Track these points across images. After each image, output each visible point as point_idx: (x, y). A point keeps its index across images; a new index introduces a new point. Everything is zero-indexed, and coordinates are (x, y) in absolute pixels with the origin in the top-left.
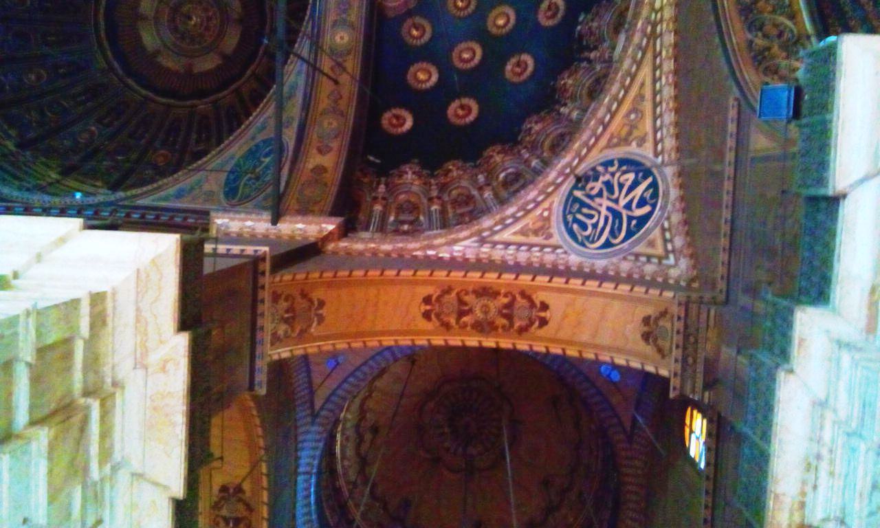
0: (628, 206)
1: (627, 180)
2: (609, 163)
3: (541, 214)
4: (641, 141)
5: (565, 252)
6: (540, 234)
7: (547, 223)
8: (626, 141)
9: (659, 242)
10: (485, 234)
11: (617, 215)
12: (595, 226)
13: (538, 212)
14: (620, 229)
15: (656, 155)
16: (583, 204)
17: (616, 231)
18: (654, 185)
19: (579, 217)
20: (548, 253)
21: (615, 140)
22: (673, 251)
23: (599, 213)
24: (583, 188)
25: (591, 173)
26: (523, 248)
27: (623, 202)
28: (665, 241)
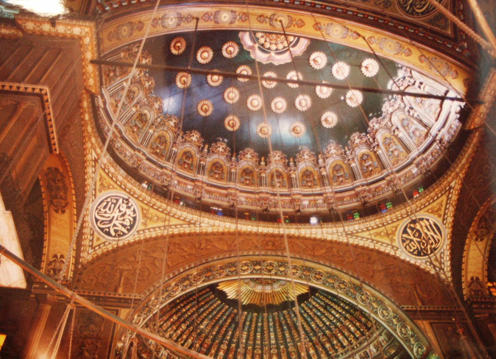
0: (115, 225)
2: (134, 211)
4: (145, 224)
8: (145, 216)
9: (99, 243)
11: (110, 221)
12: (106, 212)
14: (105, 224)
15: (138, 232)
16: (115, 204)
18: (124, 234)
19: (110, 204)
22: (95, 250)
23: (112, 213)
24: (123, 202)
25: (130, 204)
27: (117, 223)
28: (99, 245)
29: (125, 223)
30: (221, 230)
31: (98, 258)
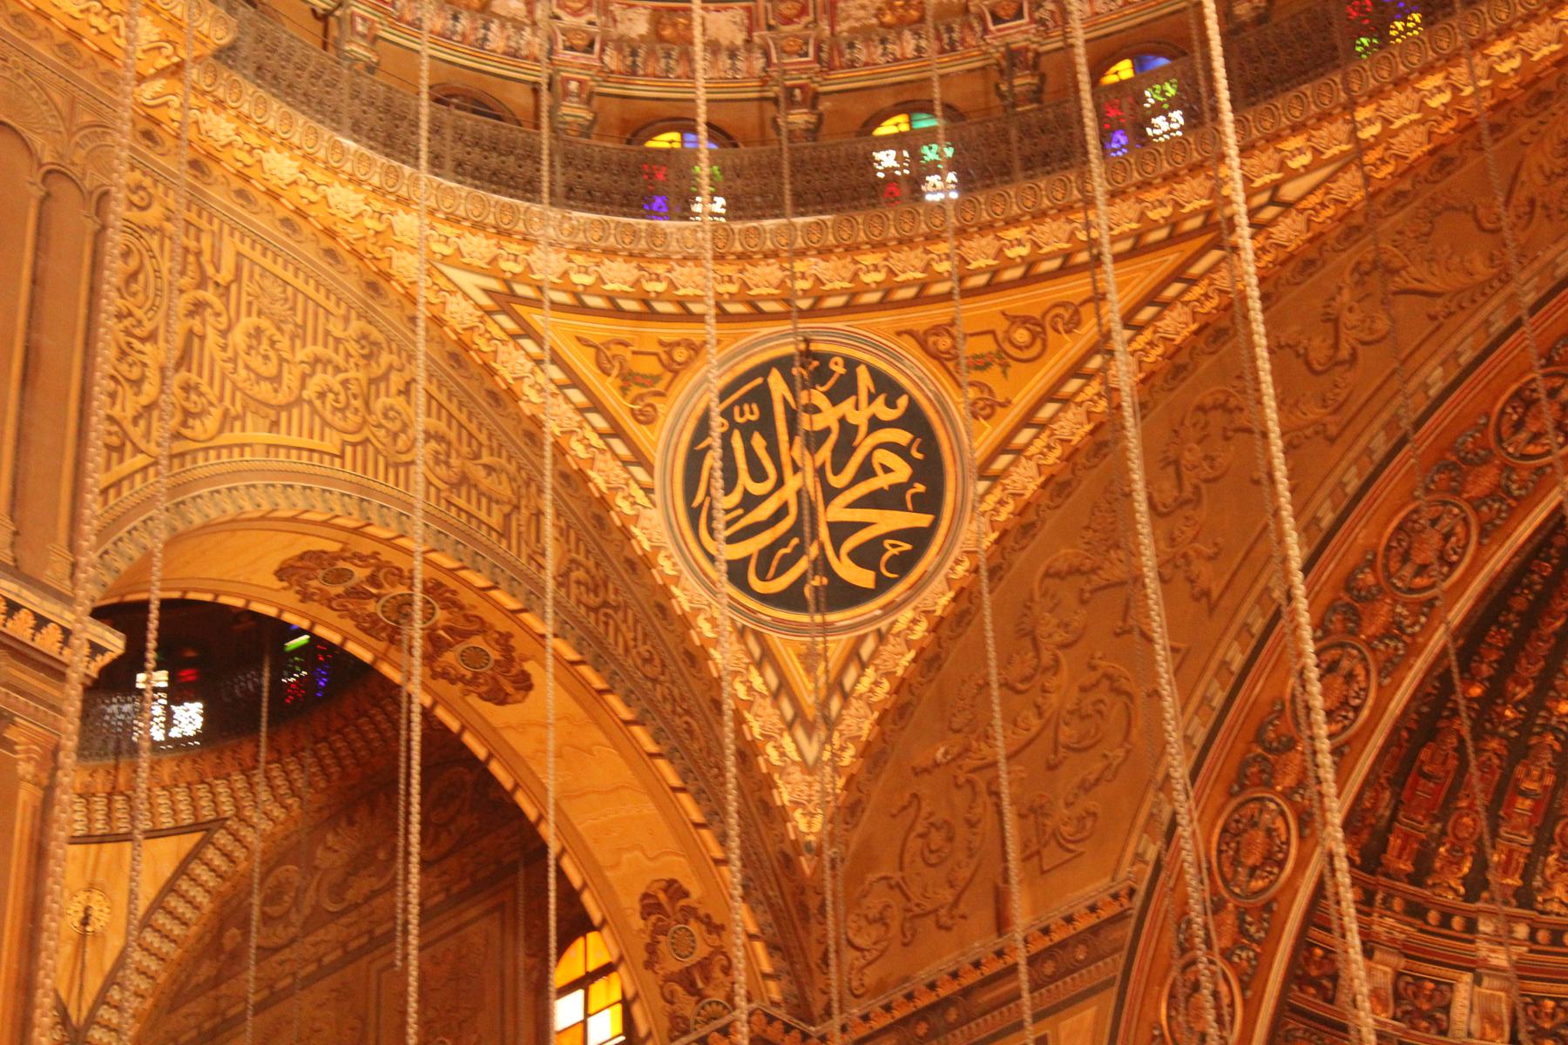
0: (841, 531)
1: (887, 470)
2: (886, 387)
3: (670, 346)
5: (648, 491)
6: (635, 390)
7: (669, 376)
10: (521, 290)
12: (750, 502)
13: (672, 332)
15: (983, 473)
16: (766, 425)
17: (775, 563)
18: (920, 539)
19: (737, 442)
20: (616, 456)
21: (944, 343)
25: (839, 368)
26: (576, 396)
27: (838, 511)
28: (836, 686)
29: (881, 481)
30: (1412, 144)
31: (874, 754)
